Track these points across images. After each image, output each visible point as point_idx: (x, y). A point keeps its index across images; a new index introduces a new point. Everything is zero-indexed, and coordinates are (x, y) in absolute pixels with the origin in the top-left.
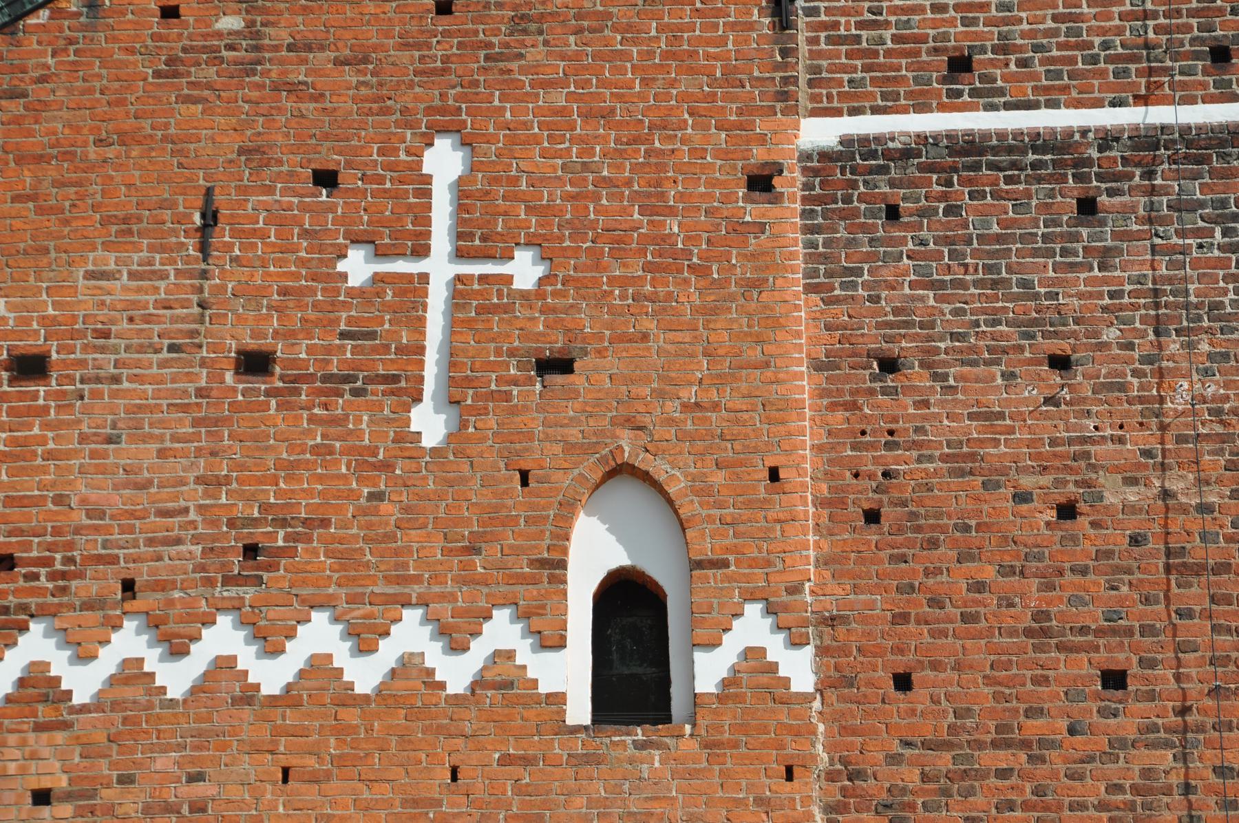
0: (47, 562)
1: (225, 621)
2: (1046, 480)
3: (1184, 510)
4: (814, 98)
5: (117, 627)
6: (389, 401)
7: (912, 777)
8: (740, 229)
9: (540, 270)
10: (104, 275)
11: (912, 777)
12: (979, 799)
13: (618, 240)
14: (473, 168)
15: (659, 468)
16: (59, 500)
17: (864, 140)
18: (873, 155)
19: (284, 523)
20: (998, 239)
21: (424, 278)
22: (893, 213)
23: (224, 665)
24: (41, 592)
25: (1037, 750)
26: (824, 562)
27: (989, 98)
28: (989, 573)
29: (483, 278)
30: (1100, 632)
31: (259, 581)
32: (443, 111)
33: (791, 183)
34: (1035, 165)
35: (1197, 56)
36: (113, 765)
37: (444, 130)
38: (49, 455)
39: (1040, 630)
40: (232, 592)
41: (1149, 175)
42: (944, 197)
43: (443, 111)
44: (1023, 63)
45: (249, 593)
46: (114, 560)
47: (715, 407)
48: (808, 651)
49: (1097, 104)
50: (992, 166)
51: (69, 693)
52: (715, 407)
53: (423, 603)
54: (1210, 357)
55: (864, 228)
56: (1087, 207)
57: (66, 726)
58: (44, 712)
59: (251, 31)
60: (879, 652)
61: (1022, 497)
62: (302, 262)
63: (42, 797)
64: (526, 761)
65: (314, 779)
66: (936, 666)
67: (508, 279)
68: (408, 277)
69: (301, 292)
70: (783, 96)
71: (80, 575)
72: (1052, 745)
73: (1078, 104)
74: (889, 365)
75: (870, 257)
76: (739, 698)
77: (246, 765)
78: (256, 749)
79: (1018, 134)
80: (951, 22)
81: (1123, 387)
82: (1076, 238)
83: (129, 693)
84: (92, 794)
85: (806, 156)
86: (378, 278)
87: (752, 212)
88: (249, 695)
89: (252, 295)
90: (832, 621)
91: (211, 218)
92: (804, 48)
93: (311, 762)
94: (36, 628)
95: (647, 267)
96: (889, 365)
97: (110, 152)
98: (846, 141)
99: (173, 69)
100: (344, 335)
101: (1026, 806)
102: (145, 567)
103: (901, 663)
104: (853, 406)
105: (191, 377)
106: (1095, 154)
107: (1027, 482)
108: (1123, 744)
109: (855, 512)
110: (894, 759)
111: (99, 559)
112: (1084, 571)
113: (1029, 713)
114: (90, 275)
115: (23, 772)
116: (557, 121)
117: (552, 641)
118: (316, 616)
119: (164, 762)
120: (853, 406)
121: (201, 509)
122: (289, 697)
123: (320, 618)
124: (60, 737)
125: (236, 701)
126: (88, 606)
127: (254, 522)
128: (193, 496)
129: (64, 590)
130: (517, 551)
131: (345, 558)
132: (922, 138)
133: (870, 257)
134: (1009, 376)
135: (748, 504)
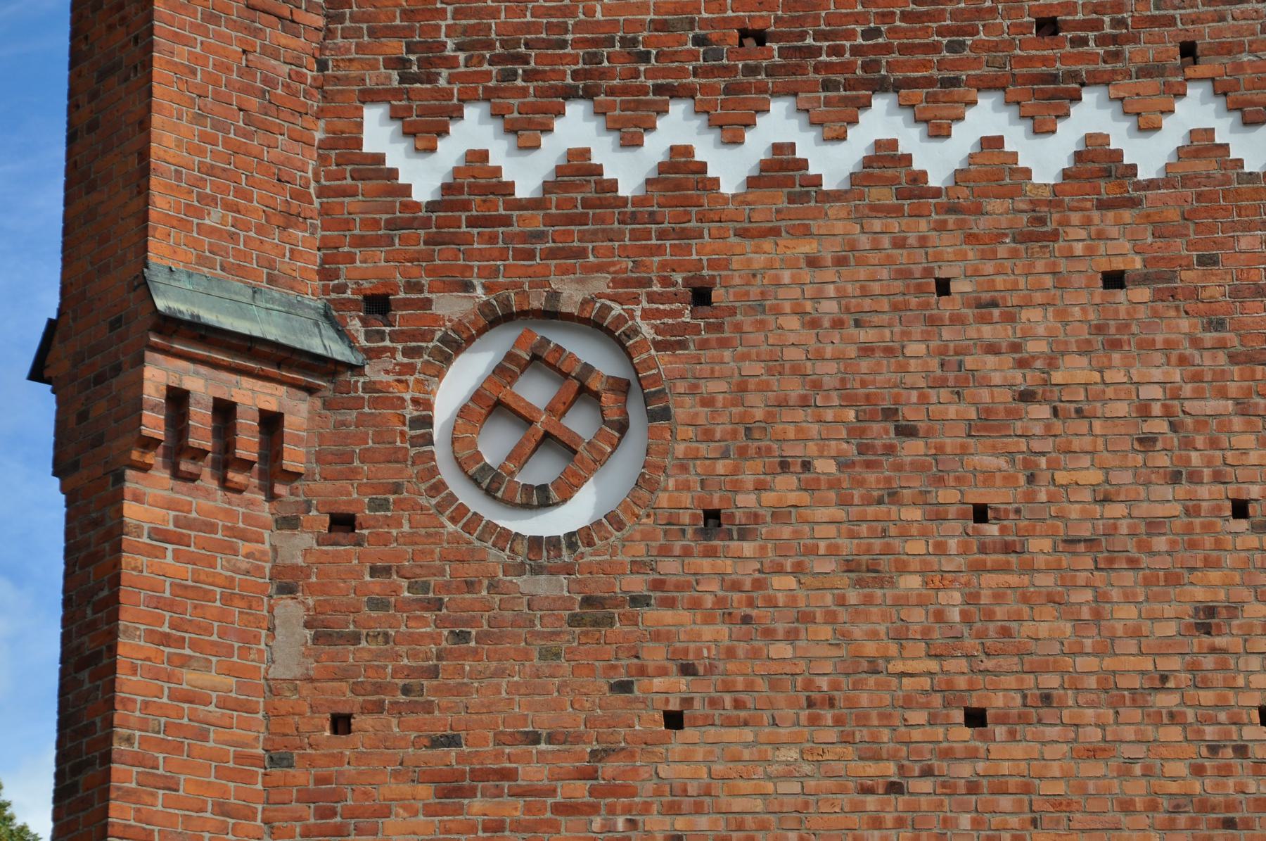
0: (1096, 25)
5: (1181, 95)
24: (1092, 57)
36: (1190, 245)
46: (1171, 21)
51: (1133, 168)
57: (1134, 203)
58: (1106, 189)
63: (1114, 280)
71: (1134, 39)
94: (1090, 96)
102: (1206, 28)
111: (1153, 21)
115: (1090, 253)
124: (1127, 215)
126: (1146, 72)
129: (1117, 56)
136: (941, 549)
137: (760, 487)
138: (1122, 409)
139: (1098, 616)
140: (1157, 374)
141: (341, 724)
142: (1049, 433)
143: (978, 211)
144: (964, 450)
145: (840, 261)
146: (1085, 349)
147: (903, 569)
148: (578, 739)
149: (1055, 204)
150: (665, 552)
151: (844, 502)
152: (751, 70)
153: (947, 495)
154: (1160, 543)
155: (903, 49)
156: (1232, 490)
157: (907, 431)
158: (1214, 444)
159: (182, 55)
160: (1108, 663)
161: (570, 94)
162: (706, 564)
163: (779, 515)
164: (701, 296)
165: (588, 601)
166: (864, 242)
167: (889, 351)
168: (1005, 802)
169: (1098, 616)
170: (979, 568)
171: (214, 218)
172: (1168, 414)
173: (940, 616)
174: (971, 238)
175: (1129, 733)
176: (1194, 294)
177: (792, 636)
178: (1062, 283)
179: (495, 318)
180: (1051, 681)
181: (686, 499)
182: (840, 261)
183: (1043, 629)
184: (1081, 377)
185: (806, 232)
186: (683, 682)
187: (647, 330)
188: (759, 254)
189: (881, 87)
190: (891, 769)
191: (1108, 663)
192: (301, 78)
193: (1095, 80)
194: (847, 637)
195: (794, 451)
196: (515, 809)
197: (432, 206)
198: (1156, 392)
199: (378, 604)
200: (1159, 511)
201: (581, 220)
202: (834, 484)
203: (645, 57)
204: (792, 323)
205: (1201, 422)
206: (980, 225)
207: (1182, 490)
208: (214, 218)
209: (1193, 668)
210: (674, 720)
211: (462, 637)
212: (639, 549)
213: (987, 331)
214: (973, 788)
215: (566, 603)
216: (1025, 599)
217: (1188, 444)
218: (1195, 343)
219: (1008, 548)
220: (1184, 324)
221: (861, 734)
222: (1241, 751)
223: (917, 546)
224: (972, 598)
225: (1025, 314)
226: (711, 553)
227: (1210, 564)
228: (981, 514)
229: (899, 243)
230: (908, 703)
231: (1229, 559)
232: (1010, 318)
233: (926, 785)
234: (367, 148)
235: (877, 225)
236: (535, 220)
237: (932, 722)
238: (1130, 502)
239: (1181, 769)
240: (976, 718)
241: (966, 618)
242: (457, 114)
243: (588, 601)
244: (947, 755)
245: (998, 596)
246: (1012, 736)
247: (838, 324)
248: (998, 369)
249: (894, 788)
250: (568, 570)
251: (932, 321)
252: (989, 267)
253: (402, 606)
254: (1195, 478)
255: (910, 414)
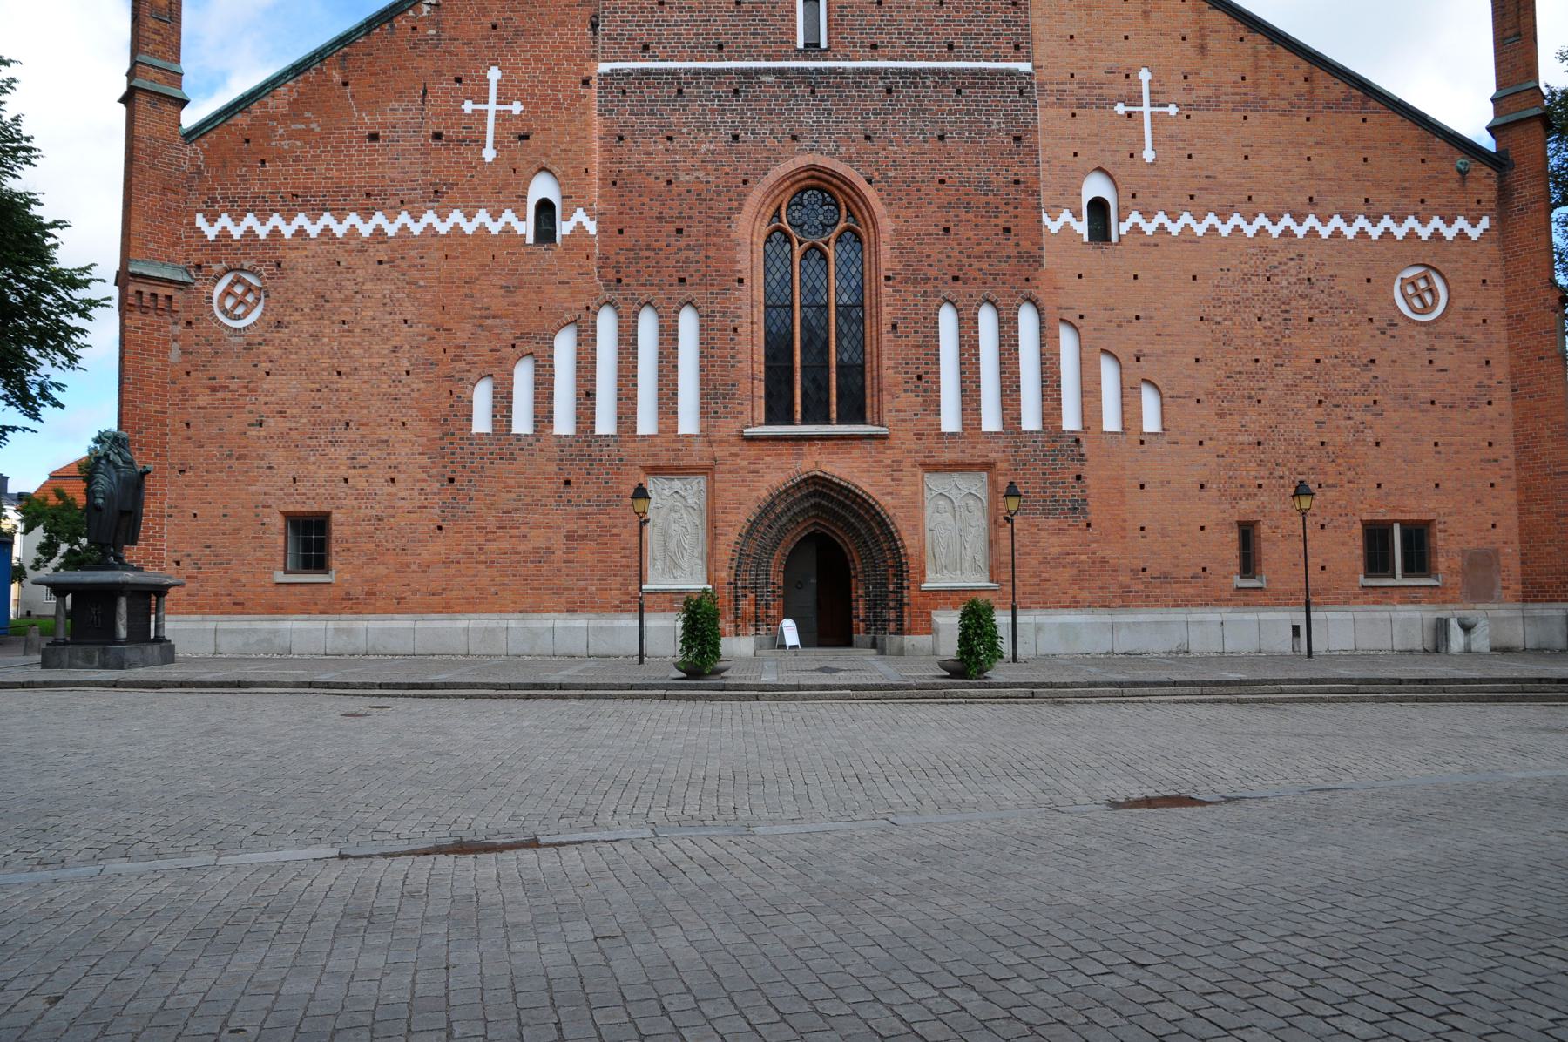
0: (380, 195)
1: (430, 212)
2: (664, 173)
3: (702, 182)
4: (603, 57)
6: (476, 148)
7: (622, 259)
8: (580, 97)
9: (522, 108)
10: (395, 110)
11: (622, 259)
12: (640, 265)
13: (544, 99)
14: (502, 76)
15: (554, 169)
16: (382, 177)
17: (617, 70)
18: (619, 74)
19: (445, 184)
20: (653, 101)
21: (487, 111)
22: (624, 92)
23: (430, 225)
25: (657, 251)
26: (600, 196)
27: (654, 57)
28: (647, 200)
29: (504, 111)
30: (677, 218)
31: (438, 201)
32: (493, 59)
33: (594, 83)
34: (666, 79)
35: (713, 47)
37: (494, 65)
38: (379, 164)
39: (660, 217)
40: (431, 204)
41: (698, 83)
42: (639, 88)
43: (493, 59)
44: (664, 48)
45: (436, 204)
47: (570, 150)
48: (595, 223)
49: (685, 61)
50: (654, 79)
52: (570, 150)
53: (485, 207)
54: (713, 138)
55: (616, 97)
56: (680, 92)
57: (386, 242)
58: (380, 239)
59: (438, 35)
60: (615, 223)
61: (657, 178)
62: (451, 106)
63: (380, 262)
64: (514, 254)
65: (455, 258)
66: (630, 227)
67: (511, 111)
68: (482, 111)
69: (451, 114)
70: (593, 56)
72: (661, 250)
73: (678, 61)
74: (621, 138)
75: (618, 106)
76: (574, 236)
77: (436, 255)
78: (438, 249)
79: (661, 69)
80: (644, 34)
81: (687, 146)
82: (676, 101)
83: (404, 233)
84: (393, 262)
85: (599, 75)
86: (474, 110)
87: (583, 91)
88: (436, 234)
89: (437, 115)
90: (602, 214)
91: (425, 92)
92: (600, 41)
93: (454, 254)
95: (552, 108)
96: (621, 138)
97: (396, 72)
98: (612, 70)
99: (415, 46)
100: (464, 128)
101: (654, 267)
102: (407, 197)
103: (621, 226)
104: (611, 151)
105: (419, 140)
106: (683, 76)
107: (658, 174)
108: (680, 249)
109: (610, 182)
110: (618, 254)
112: (673, 200)
113: (657, 241)
114: (391, 110)
116: (526, 63)
117: (523, 219)
118: (455, 211)
119: (413, 253)
120: (611, 151)
121: (422, 180)
122: (448, 235)
123: (456, 212)
124: (384, 245)
125: (433, 236)
126: (391, 208)
127: (437, 184)
128: (420, 176)
129: (384, 204)
130: (512, 193)
131: (464, 195)
132: (633, 70)
133: (618, 106)
134: (655, 142)
135: (579, 179)
136: (333, 331)
137: (291, 315)
138: (379, 296)
139: (369, 348)
140: (388, 287)
141: (188, 373)
142: (361, 302)
143: (348, 244)
144: (341, 306)
145: (314, 257)
146: (372, 280)
147: (324, 336)
148: (244, 378)
149: (368, 242)
150: (267, 332)
151: (311, 319)
152: (294, 205)
153: (334, 318)
154: (386, 330)
155: (333, 200)
156: (403, 317)
157: (327, 301)
158: (400, 305)
159: (141, 203)
160: (371, 360)
161: (248, 211)
162: (276, 335)
163: (295, 323)
164: (279, 265)
165: (248, 344)
166: (319, 251)
167: (324, 281)
168: (344, 394)
169: (369, 348)
170: (342, 336)
171: (151, 246)
172: (390, 297)
173: (332, 348)
174: (346, 251)
175: (374, 377)
176: (398, 266)
177: (296, 353)
178: (367, 263)
179: (228, 271)
180: (357, 364)
181: (272, 318)
182: (314, 257)
183: (356, 352)
184: (370, 287)
185: (305, 248)
186: (270, 365)
187: (265, 274)
188: (292, 255)
189: (326, 210)
190: (318, 386)
191: (371, 360)
192: (180, 207)
193: (379, 210)
194: (309, 354)
195: (299, 306)
196: (228, 395)
197: (213, 241)
198: (388, 292)
199: (197, 344)
200: (386, 322)
201: (250, 245)
202: (309, 315)
203: (267, 201)
204: (300, 272)
205: (398, 300)
206: (348, 247)
207: (391, 317)
208: (151, 246)
209: (391, 361)
210: (268, 374)
211: (217, 353)
212: (261, 331)
213: (348, 276)
214: (337, 391)
215: (242, 344)
216: (353, 344)
217: (394, 305)
218: (398, 279)
219: (349, 331)
220: (396, 274)
221: (312, 377)
222: (400, 381)
223: (327, 331)
224: (340, 344)
225: (358, 271)
226: (278, 332)
227: (397, 335)
228: (344, 322)
229: (328, 252)
230: (323, 370)
231: (402, 334)
232: (354, 272)
233: (326, 390)
234: (197, 225)
235: (323, 247)
236: (238, 245)
237: (329, 374)
238: (380, 320)
239: (386, 386)
240: (339, 373)
241: (338, 349)
242: (220, 216)
243: (248, 344)
244: (332, 382)
245: (346, 344)
246: (347, 378)
247: (312, 273)
248: (351, 286)
249: (319, 391)
250: (243, 336)
251: (336, 273)
252: (350, 258)
253: (204, 345)
254: (395, 314)
255: (327, 297)
